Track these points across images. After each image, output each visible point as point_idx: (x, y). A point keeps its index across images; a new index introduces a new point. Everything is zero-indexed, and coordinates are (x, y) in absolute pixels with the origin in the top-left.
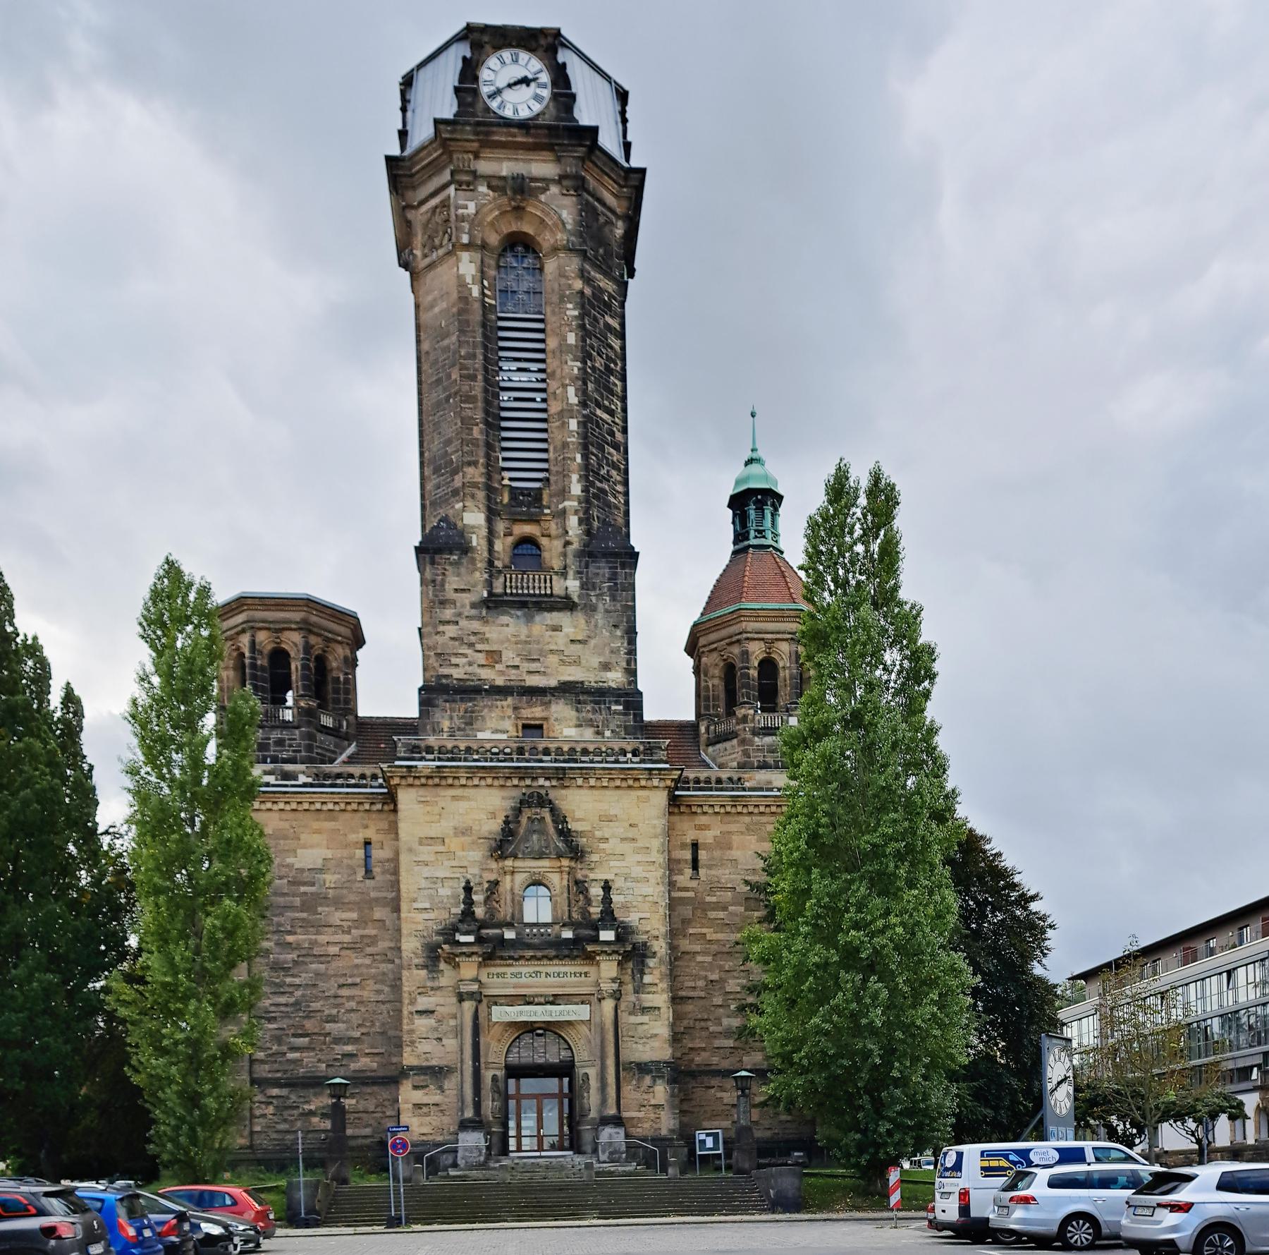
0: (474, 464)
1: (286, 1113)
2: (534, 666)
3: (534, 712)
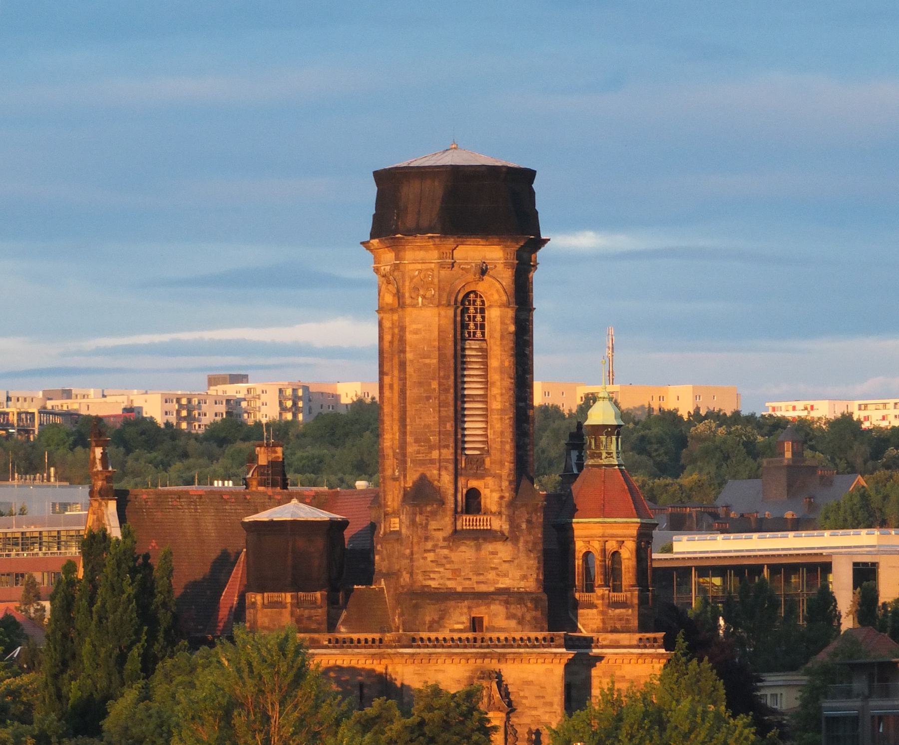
0: (447, 447)
2: (481, 578)
3: (480, 611)
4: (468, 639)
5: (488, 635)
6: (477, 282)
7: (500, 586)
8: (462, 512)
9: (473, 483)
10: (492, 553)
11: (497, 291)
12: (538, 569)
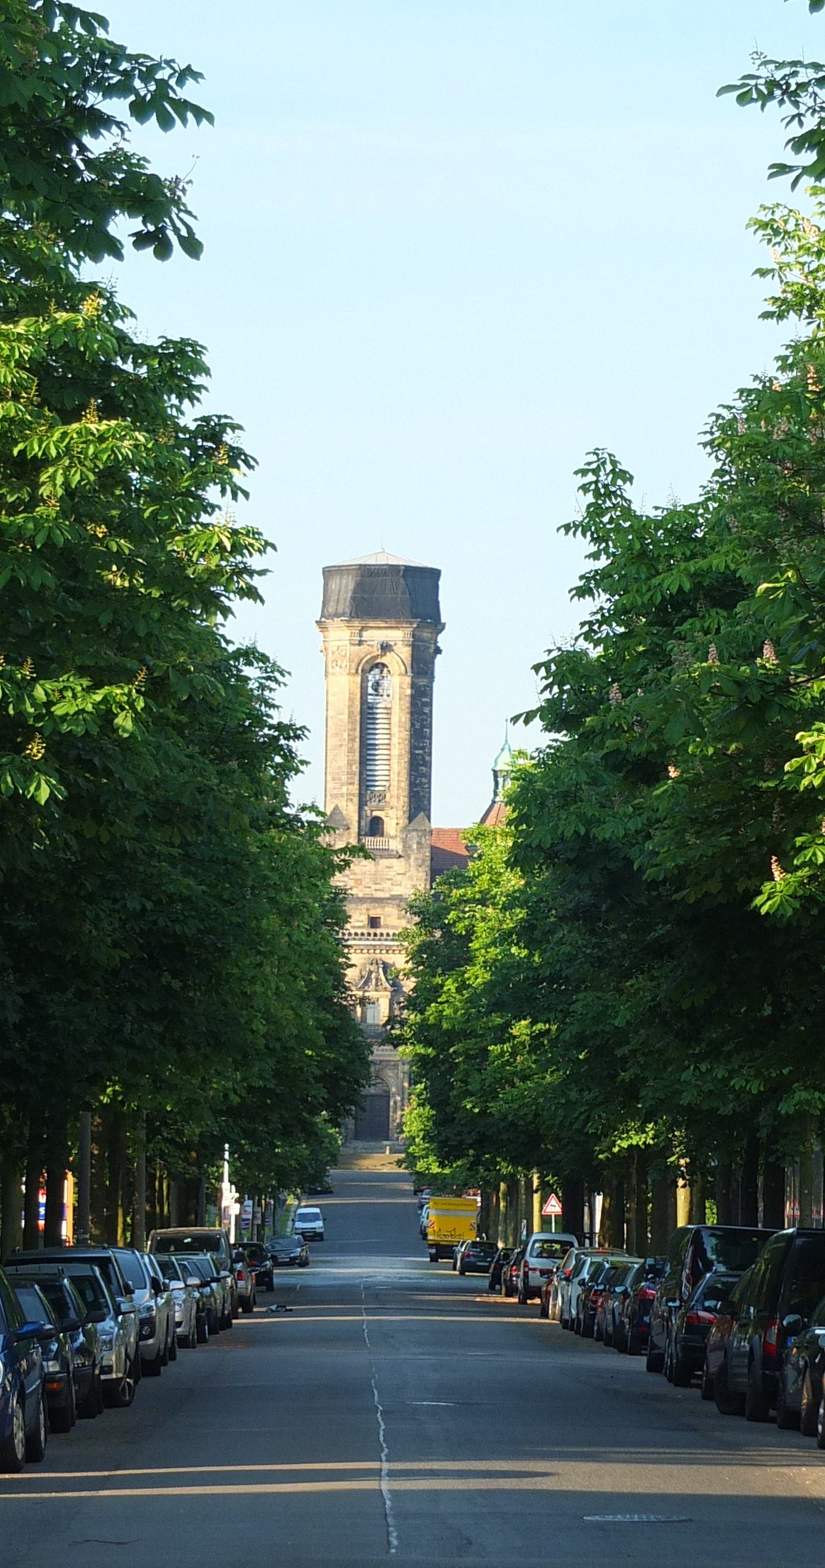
0: (353, 784)
2: (378, 887)
4: (363, 934)
5: (385, 932)
6: (382, 656)
7: (394, 893)
8: (366, 835)
9: (375, 813)
10: (388, 867)
11: (397, 663)
12: (426, 880)
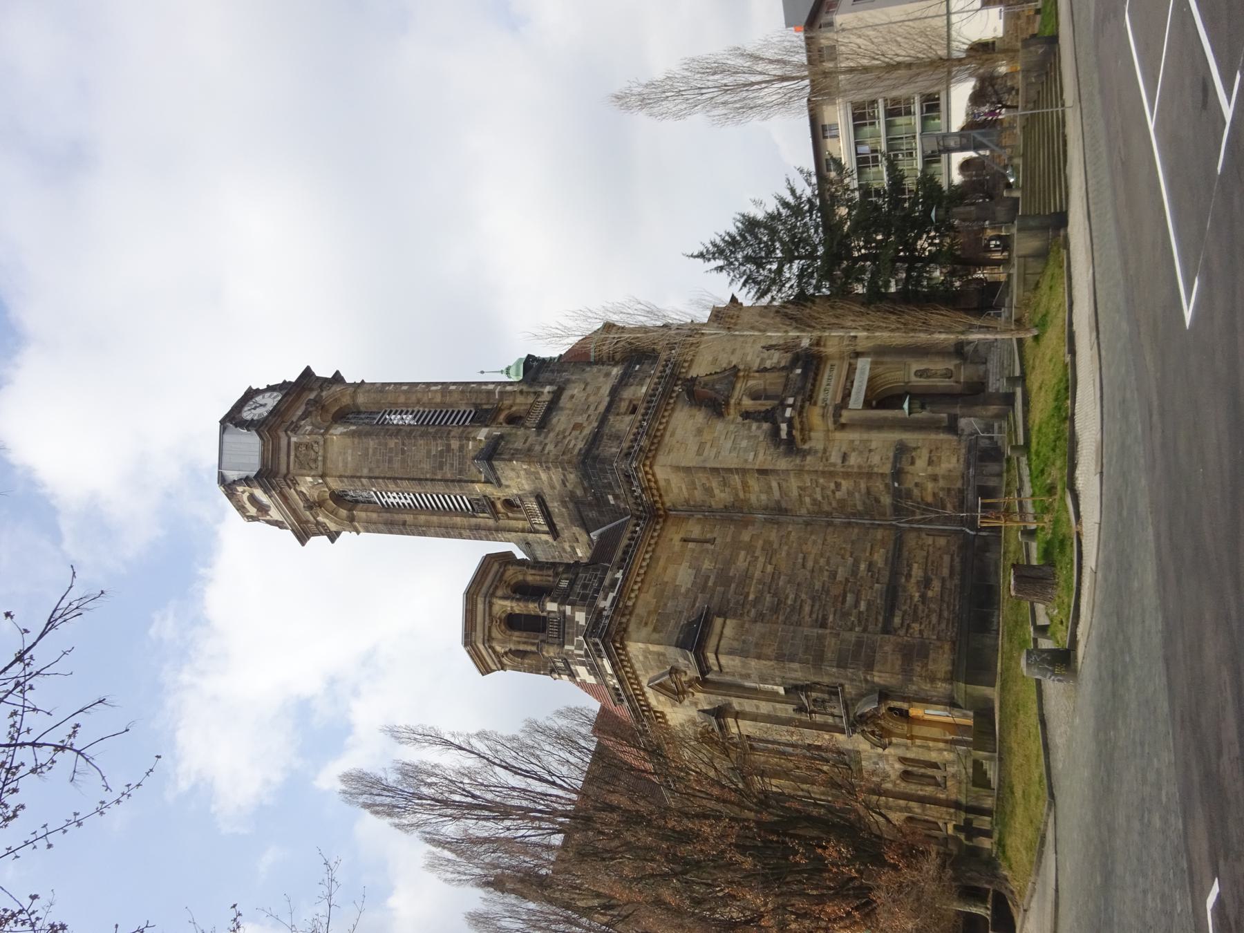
1: (920, 614)
2: (592, 408)
